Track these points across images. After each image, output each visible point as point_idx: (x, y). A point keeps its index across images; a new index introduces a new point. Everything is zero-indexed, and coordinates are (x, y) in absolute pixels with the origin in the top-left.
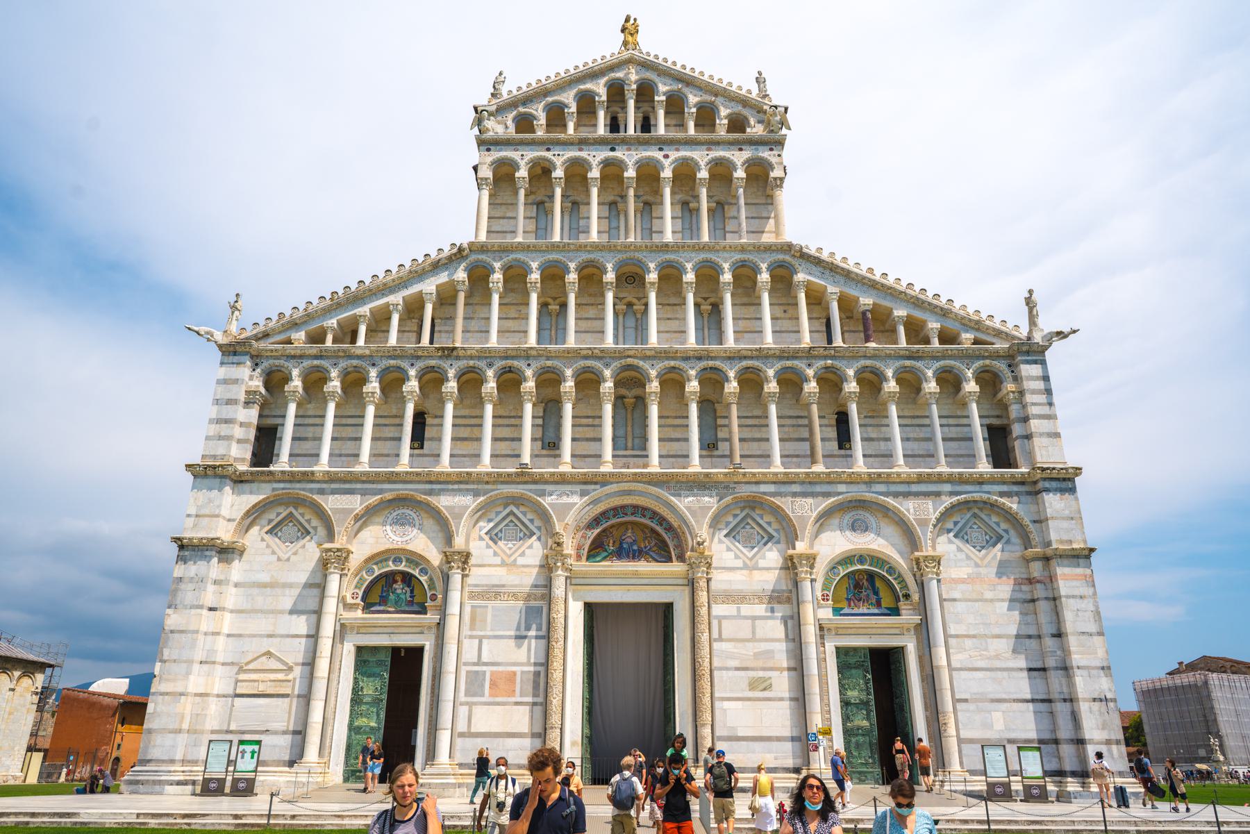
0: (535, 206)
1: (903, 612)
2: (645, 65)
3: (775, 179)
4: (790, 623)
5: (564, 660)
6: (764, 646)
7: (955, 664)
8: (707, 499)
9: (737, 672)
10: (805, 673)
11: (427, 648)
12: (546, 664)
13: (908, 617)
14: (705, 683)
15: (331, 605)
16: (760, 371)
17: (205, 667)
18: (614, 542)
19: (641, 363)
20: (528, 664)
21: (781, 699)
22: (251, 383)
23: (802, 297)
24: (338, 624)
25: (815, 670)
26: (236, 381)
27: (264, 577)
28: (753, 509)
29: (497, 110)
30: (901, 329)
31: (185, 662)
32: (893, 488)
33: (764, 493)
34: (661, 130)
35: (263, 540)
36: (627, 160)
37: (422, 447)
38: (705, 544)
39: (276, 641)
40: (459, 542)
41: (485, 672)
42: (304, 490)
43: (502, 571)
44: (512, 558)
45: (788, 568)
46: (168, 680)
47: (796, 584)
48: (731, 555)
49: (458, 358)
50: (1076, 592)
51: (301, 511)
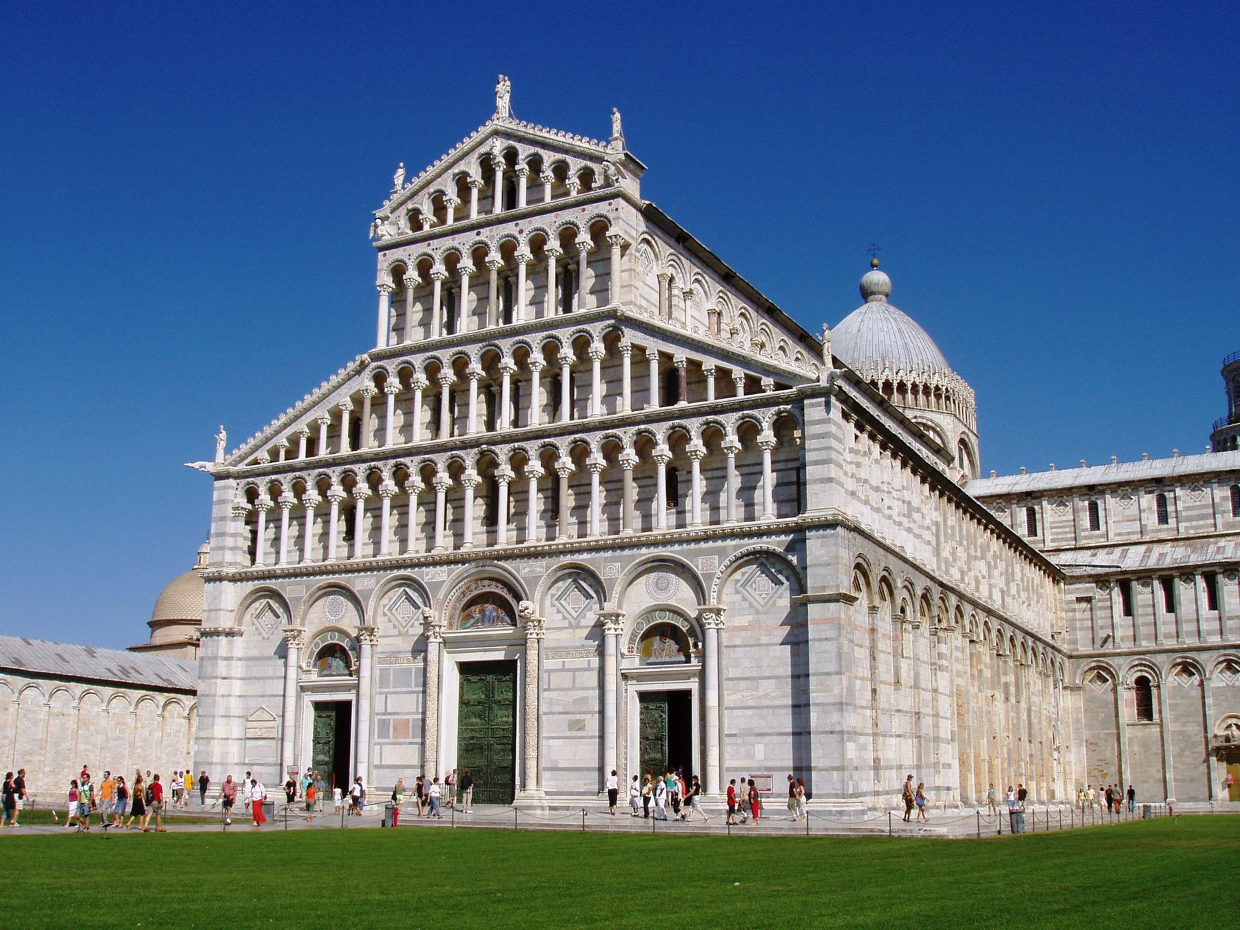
2: (507, 135)
3: (610, 237)
6: (580, 694)
8: (538, 569)
15: (292, 673)
17: (225, 719)
22: (236, 501)
27: (255, 653)
29: (392, 211)
30: (711, 381)
33: (583, 560)
36: (489, 243)
38: (526, 612)
42: (272, 584)
43: (398, 640)
46: (203, 729)
48: (560, 616)
49: (364, 461)
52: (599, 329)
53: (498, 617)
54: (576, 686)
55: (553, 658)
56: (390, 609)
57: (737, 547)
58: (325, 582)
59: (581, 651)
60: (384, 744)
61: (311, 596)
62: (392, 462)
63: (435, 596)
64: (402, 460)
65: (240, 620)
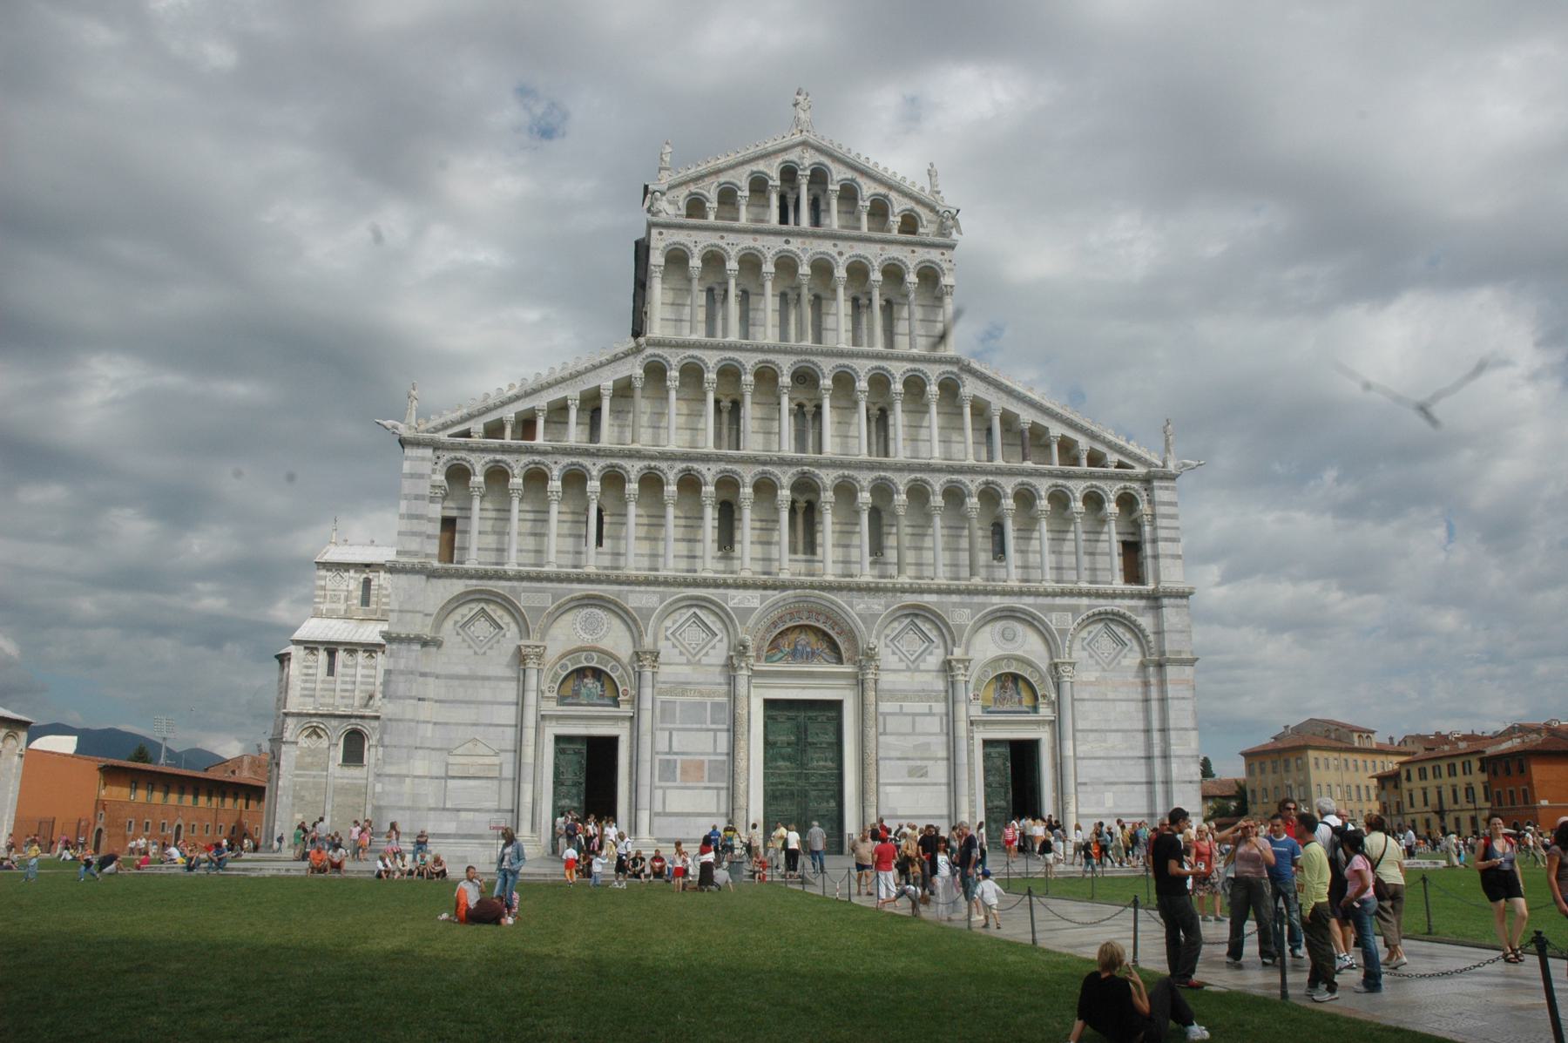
0: (704, 294)
1: (1041, 710)
2: (819, 150)
3: (946, 286)
4: (944, 719)
5: (748, 750)
6: (922, 739)
7: (1079, 754)
8: (876, 607)
9: (899, 762)
10: (958, 762)
11: (621, 739)
12: (732, 753)
13: (1045, 712)
14: (871, 770)
15: (531, 698)
16: (927, 483)
17: (420, 752)
18: (789, 644)
19: (817, 471)
20: (715, 753)
21: (935, 784)
23: (967, 411)
24: (539, 716)
25: (965, 761)
26: (421, 476)
27: (462, 670)
28: (917, 615)
29: (669, 189)
31: (405, 747)
32: (1041, 600)
33: (928, 603)
34: (834, 220)
35: (458, 634)
36: (801, 255)
37: (601, 545)
39: (481, 729)
40: (648, 642)
41: (675, 761)
42: (496, 587)
43: (687, 670)
44: (697, 658)
45: (946, 671)
46: (391, 764)
47: (952, 684)
48: (896, 658)
50: (1181, 695)
51: (492, 607)
52: (937, 373)
53: (813, 653)
54: (917, 731)
55: (888, 701)
56: (673, 634)
57: (1089, 607)
58: (584, 593)
59: (924, 695)
60: (668, 788)
61: (559, 607)
62: (681, 466)
63: (743, 623)
64: (695, 466)
65: (438, 624)
